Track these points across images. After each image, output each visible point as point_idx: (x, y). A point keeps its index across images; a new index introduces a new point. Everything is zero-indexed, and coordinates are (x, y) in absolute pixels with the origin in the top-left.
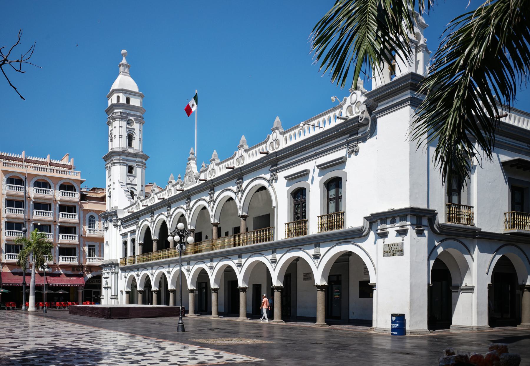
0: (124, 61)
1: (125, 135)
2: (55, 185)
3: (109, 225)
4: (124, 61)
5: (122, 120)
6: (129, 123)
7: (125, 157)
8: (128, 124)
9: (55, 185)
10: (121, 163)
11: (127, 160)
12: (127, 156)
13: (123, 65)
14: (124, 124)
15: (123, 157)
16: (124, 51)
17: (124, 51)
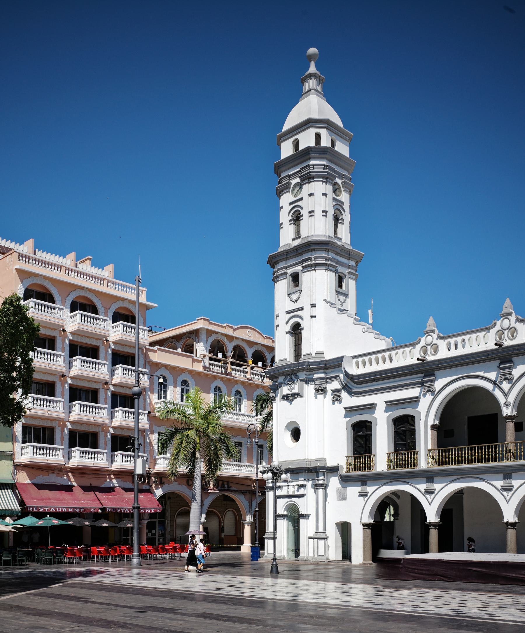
0: (312, 69)
1: (331, 212)
2: (107, 309)
3: (301, 388)
4: (312, 69)
5: (326, 182)
6: (336, 190)
7: (334, 255)
8: (335, 191)
9: (107, 309)
10: (329, 265)
11: (338, 262)
12: (337, 254)
13: (310, 76)
14: (329, 189)
15: (331, 255)
16: (313, 50)
17: (313, 50)
